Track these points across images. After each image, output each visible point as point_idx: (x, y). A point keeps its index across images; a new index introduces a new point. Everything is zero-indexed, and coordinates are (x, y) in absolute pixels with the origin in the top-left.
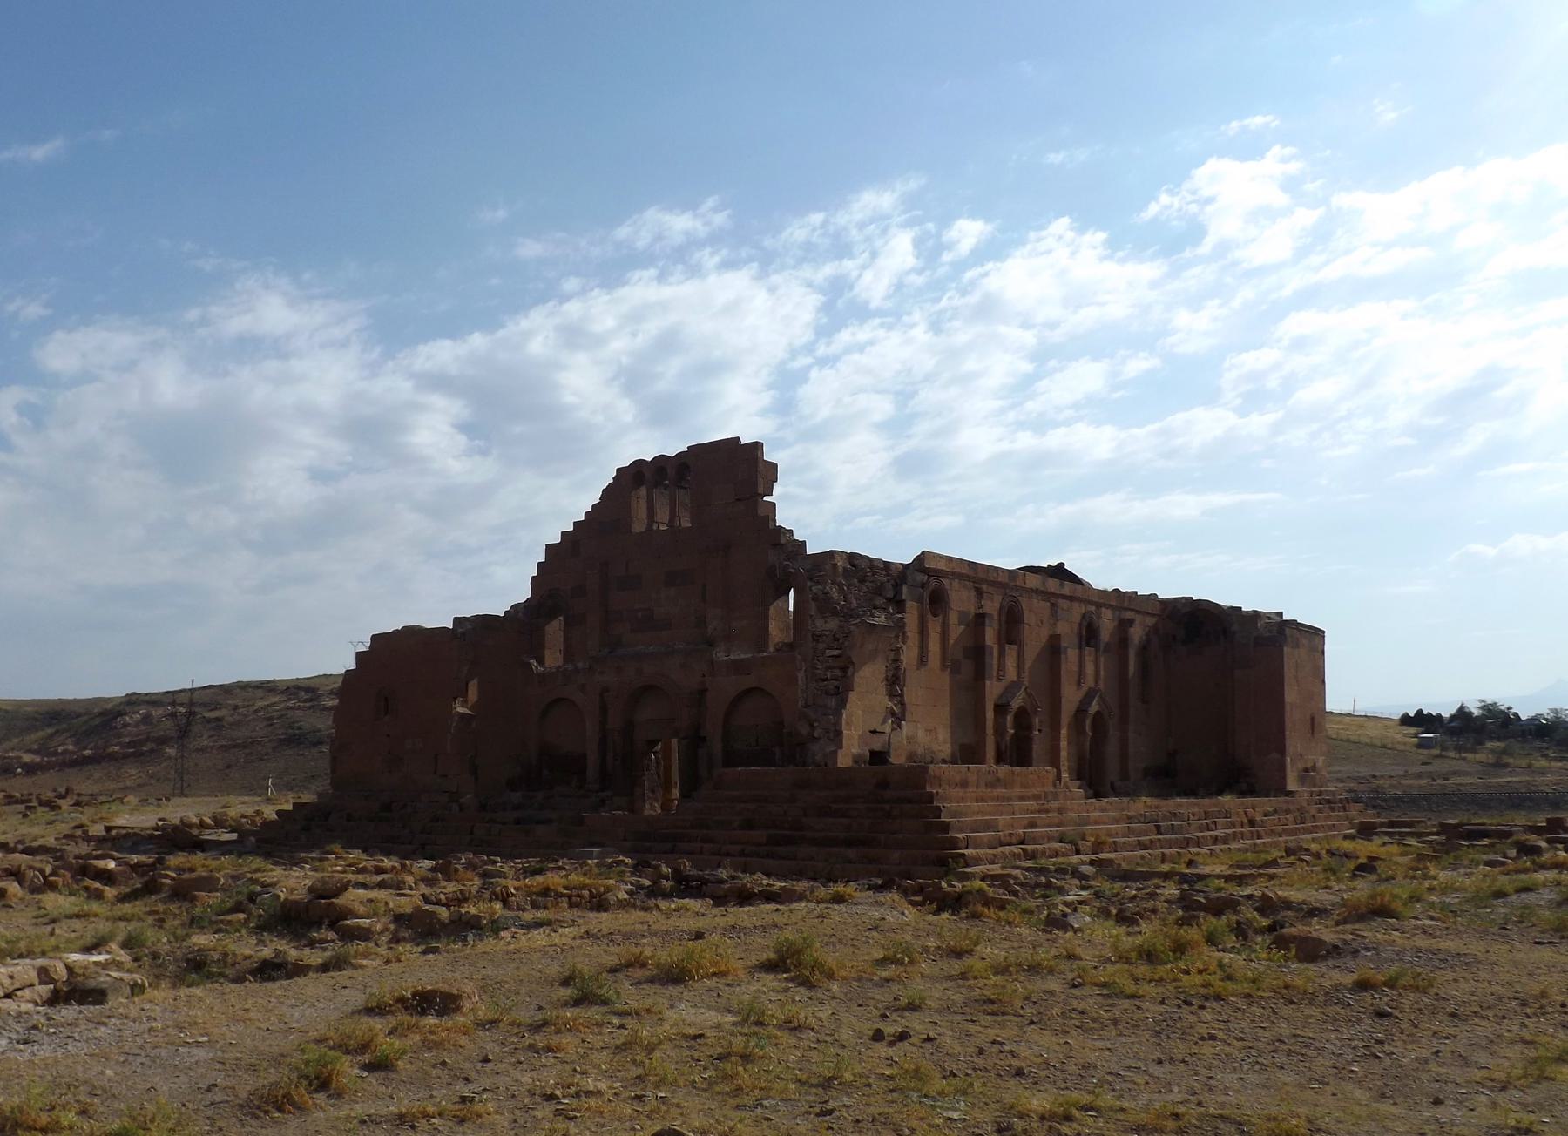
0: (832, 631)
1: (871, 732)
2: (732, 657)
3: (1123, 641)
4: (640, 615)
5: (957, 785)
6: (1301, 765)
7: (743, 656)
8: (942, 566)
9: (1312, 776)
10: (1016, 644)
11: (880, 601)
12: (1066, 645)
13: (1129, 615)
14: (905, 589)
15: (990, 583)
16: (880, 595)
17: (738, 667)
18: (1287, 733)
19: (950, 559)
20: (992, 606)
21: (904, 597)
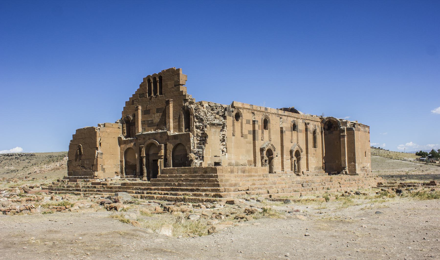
1: (215, 156)
3: (306, 130)
6: (362, 166)
9: (365, 169)
10: (268, 129)
12: (285, 130)
13: (307, 121)
14: (226, 112)
15: (257, 111)
17: (175, 137)
20: (259, 118)
21: (226, 115)
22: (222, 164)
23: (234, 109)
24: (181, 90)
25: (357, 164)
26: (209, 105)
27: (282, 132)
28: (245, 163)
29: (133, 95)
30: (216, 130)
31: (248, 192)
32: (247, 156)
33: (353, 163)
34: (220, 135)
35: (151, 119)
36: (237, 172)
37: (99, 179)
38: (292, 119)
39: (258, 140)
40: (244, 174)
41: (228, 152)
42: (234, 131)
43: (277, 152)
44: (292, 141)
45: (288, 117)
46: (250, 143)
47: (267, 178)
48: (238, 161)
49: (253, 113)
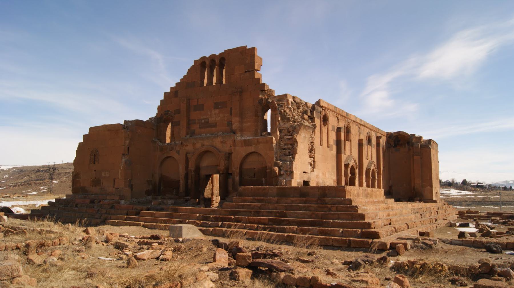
0: (287, 128)
4: (203, 121)
7: (248, 138)
8: (326, 106)
10: (349, 141)
11: (306, 116)
13: (379, 135)
14: (315, 112)
17: (247, 143)
18: (433, 179)
19: (328, 104)
21: (314, 116)
23: (322, 109)
24: (256, 77)
25: (433, 189)
26: (295, 101)
28: (331, 184)
29: (176, 84)
30: (306, 136)
33: (429, 187)
35: (206, 118)
41: (316, 167)
42: (321, 138)
45: (365, 128)
48: (325, 181)
49: (337, 117)
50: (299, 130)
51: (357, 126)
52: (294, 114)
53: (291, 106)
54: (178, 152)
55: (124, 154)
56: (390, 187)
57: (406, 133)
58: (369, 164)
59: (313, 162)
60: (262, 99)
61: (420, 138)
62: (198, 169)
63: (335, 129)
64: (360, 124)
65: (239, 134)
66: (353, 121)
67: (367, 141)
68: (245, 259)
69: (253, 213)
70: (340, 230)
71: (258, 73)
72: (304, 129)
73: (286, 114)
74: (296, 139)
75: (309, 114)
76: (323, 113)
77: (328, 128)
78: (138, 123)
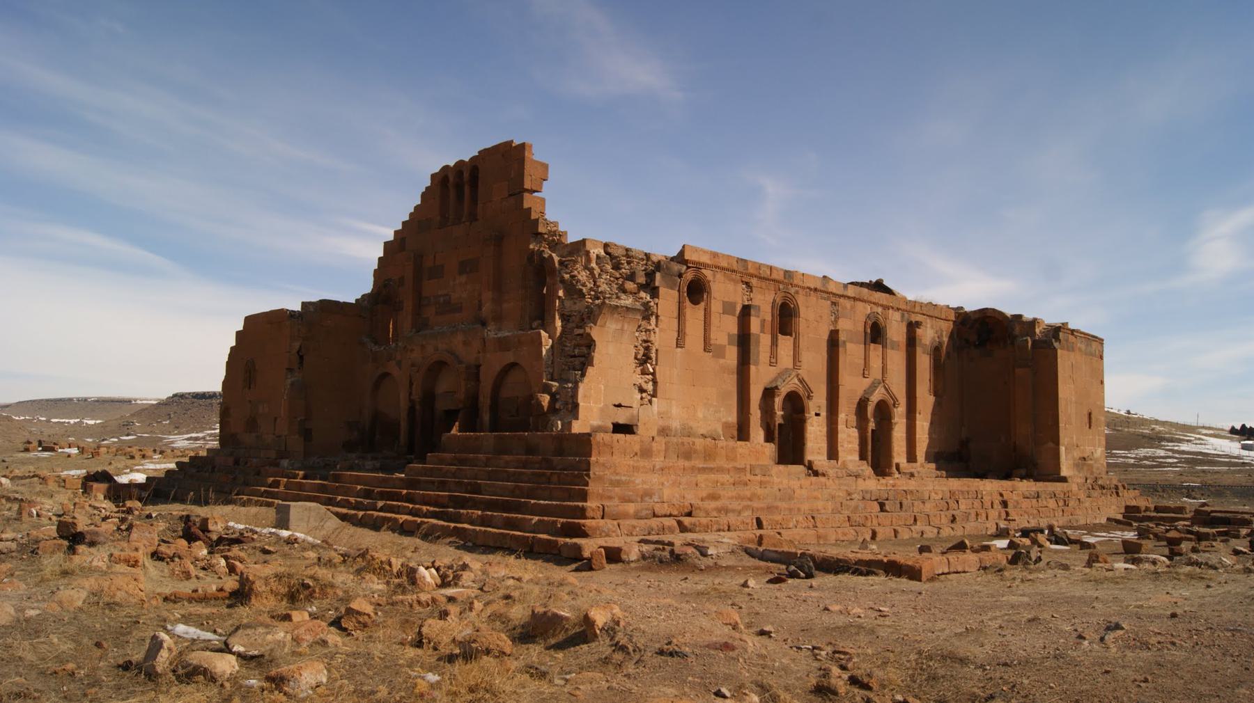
0: (580, 312)
1: (615, 405)
2: (499, 335)
3: (911, 342)
4: (442, 299)
5: (636, 454)
6: (1077, 454)
7: (507, 334)
8: (705, 259)
10: (791, 335)
11: (630, 286)
13: (915, 318)
14: (658, 275)
16: (632, 281)
17: (503, 345)
18: (1061, 425)
19: (715, 255)
20: (764, 302)
22: (641, 430)
23: (685, 267)
24: (526, 206)
25: (1062, 449)
26: (607, 253)
27: (834, 343)
29: (404, 223)
30: (623, 326)
31: (687, 521)
32: (722, 409)
33: (1051, 445)
34: (636, 344)
36: (662, 454)
37: (287, 461)
38: (868, 309)
39: (757, 364)
40: (687, 464)
41: (658, 395)
43: (817, 403)
44: (866, 372)
46: (733, 373)
47: (763, 479)
48: (691, 424)
49: (747, 284)
50: (599, 315)
51: (828, 299)
52: (601, 281)
53: (597, 264)
54: (399, 364)
55: (290, 370)
56: (964, 444)
57: (1001, 313)
58: (870, 387)
59: (651, 383)
60: (533, 251)
61: (1034, 322)
62: (429, 397)
63: (735, 310)
64: (834, 294)
65: (492, 326)
66: (809, 288)
67: (865, 333)
68: (68, 526)
69: (436, 484)
70: (532, 519)
71: (536, 197)
72: (612, 314)
73: (577, 282)
74: (589, 335)
75: (641, 279)
76: (689, 276)
77: (705, 309)
78: (327, 307)
